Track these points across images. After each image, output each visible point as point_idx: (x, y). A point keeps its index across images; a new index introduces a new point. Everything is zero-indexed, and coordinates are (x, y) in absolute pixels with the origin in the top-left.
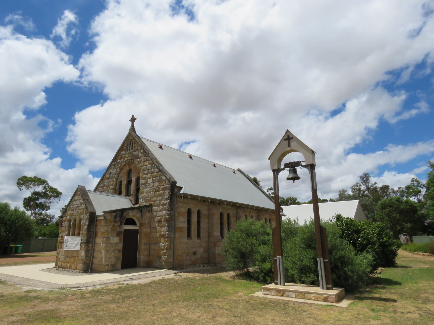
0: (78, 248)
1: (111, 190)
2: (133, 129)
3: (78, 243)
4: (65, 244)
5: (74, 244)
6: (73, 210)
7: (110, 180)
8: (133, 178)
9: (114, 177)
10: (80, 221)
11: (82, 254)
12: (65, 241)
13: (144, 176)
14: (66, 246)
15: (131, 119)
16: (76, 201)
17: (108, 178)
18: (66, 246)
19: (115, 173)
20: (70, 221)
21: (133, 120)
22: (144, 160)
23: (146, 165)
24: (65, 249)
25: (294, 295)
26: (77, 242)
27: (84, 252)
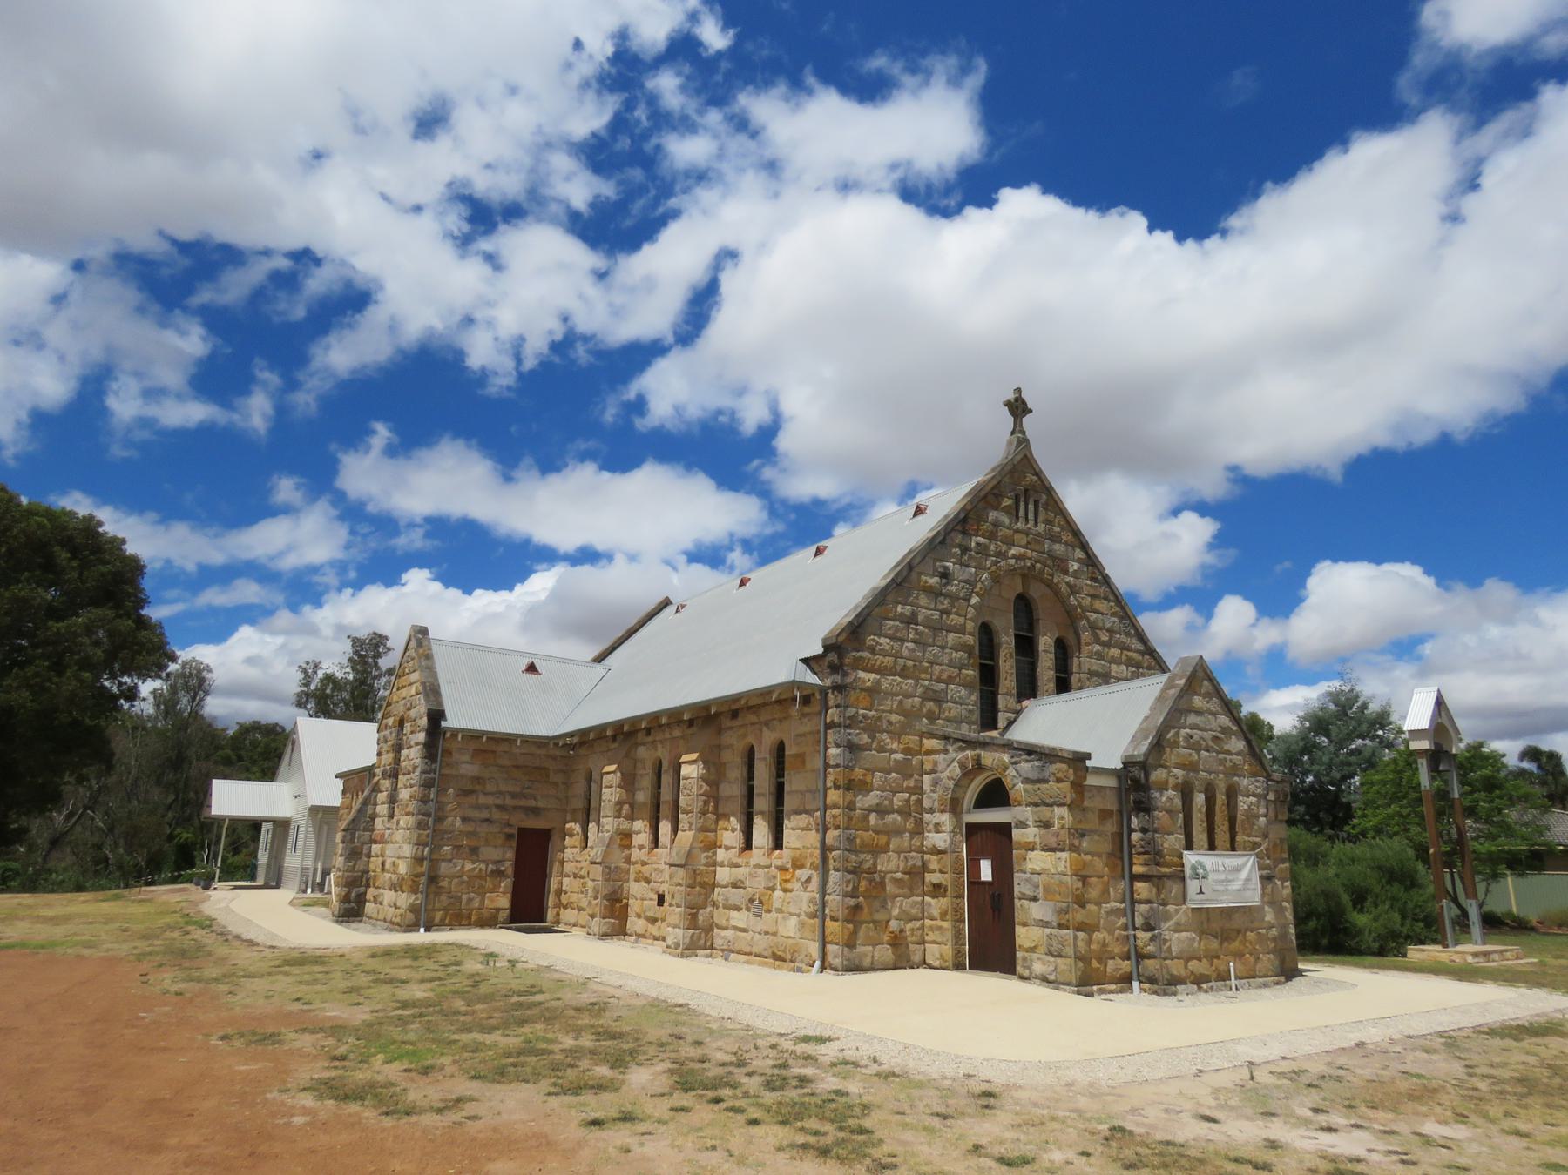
0: (1254, 897)
2: (1021, 441)
3: (1248, 879)
4: (1192, 886)
5: (1233, 880)
9: (967, 599)
10: (1232, 793)
11: (1267, 919)
13: (1098, 647)
14: (1201, 892)
15: (1024, 403)
16: (1198, 712)
17: (934, 593)
18: (1201, 892)
19: (967, 582)
20: (1186, 792)
21: (1018, 408)
22: (1092, 592)
23: (1101, 610)
24: (1194, 900)
25: (1496, 957)
26: (1244, 874)
27: (1270, 910)
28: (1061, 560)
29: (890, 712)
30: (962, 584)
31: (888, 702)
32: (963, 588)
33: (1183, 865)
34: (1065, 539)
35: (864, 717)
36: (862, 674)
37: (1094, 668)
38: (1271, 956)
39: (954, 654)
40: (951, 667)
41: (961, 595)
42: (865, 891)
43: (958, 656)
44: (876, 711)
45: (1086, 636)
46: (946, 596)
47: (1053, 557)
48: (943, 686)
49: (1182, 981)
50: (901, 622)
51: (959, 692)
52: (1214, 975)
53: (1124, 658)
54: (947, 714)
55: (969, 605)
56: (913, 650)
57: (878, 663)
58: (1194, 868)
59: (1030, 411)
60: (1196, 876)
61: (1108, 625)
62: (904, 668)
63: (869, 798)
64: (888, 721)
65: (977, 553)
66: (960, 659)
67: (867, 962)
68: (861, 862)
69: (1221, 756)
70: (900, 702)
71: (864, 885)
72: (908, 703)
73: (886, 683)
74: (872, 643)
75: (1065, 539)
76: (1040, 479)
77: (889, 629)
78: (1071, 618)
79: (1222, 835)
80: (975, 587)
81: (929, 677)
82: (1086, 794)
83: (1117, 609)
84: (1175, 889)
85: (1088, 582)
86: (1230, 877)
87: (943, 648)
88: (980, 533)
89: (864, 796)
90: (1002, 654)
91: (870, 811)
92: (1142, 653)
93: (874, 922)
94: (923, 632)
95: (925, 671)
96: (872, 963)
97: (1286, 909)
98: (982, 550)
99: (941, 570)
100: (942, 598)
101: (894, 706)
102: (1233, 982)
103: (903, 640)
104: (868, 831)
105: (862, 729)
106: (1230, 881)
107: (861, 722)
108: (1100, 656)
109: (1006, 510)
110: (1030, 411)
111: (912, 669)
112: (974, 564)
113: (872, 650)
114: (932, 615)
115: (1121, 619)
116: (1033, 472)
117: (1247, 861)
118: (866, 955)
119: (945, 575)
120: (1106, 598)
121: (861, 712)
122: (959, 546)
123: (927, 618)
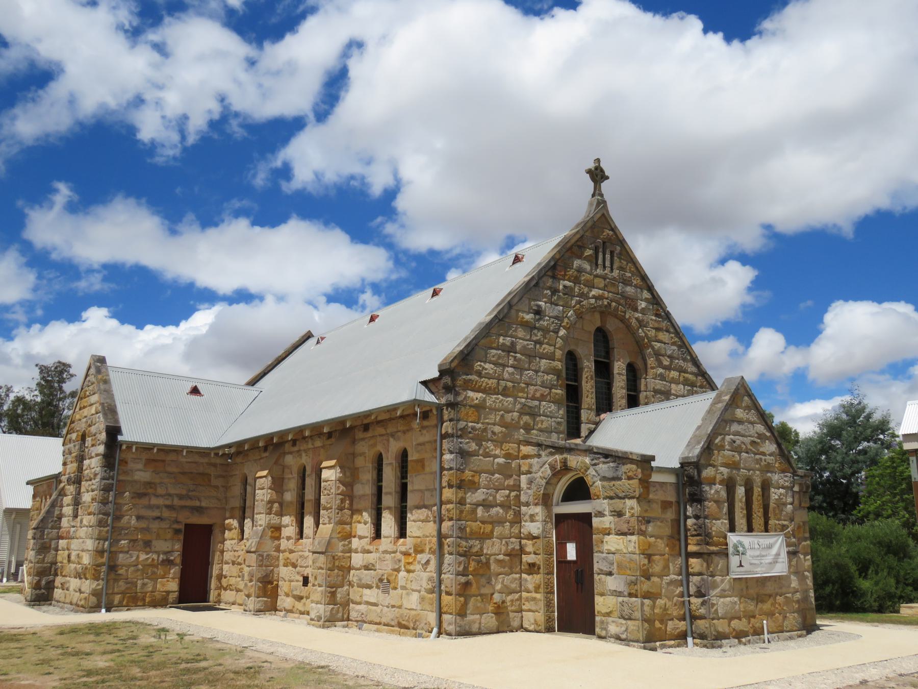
0: (781, 568)
1: (548, 374)
2: (601, 203)
3: (778, 554)
4: (734, 560)
5: (766, 556)
6: (738, 450)
7: (539, 335)
8: (619, 360)
9: (556, 332)
10: (766, 486)
11: (792, 585)
12: (731, 550)
13: (661, 370)
15: (602, 171)
16: (740, 422)
18: (741, 566)
19: (556, 318)
20: (730, 486)
21: (597, 175)
22: (656, 325)
23: (664, 340)
26: (774, 551)
27: (795, 578)
28: (632, 300)
29: (494, 424)
30: (552, 320)
31: (492, 416)
32: (553, 323)
33: (727, 544)
34: (635, 282)
35: (472, 429)
36: (471, 394)
37: (658, 387)
38: (796, 615)
39: (546, 377)
40: (543, 387)
41: (552, 328)
42: (474, 570)
43: (549, 378)
44: (482, 423)
45: (651, 361)
46: (539, 329)
47: (624, 296)
48: (537, 403)
49: (726, 637)
50: (503, 351)
51: (550, 407)
52: (751, 631)
53: (681, 379)
54: (540, 425)
55: (557, 337)
56: (513, 374)
57: (484, 384)
58: (735, 547)
59: (607, 178)
60: (737, 553)
61: (669, 352)
62: (505, 388)
63: (477, 494)
64: (492, 432)
65: (565, 294)
66: (551, 380)
67: (475, 628)
68: (471, 547)
69: (758, 457)
70: (502, 416)
71: (473, 565)
72: (508, 417)
73: (490, 400)
74: (479, 368)
75: (635, 282)
76: (615, 233)
77: (493, 356)
78: (640, 347)
79: (758, 521)
80: (562, 321)
81: (525, 395)
82: (652, 489)
83: (676, 339)
84: (720, 563)
85: (654, 318)
86: (764, 553)
87: (537, 372)
88: (567, 278)
89: (473, 493)
90: (584, 376)
91: (477, 505)
92: (696, 375)
93: (481, 595)
94: (520, 359)
95: (522, 390)
96: (480, 628)
97: (807, 577)
98: (568, 292)
99: (535, 308)
100: (536, 331)
101: (497, 420)
102: (766, 636)
103: (504, 366)
104: (476, 521)
105: (471, 439)
106: (763, 556)
107: (470, 433)
108: (662, 378)
109: (587, 259)
110: (607, 178)
111: (511, 389)
112: (561, 303)
113: (479, 374)
114: (528, 345)
115: (680, 347)
116: (609, 228)
117: (778, 540)
118: (474, 622)
119: (538, 312)
120: (667, 331)
121: (470, 424)
122: (550, 288)
123: (524, 347)
